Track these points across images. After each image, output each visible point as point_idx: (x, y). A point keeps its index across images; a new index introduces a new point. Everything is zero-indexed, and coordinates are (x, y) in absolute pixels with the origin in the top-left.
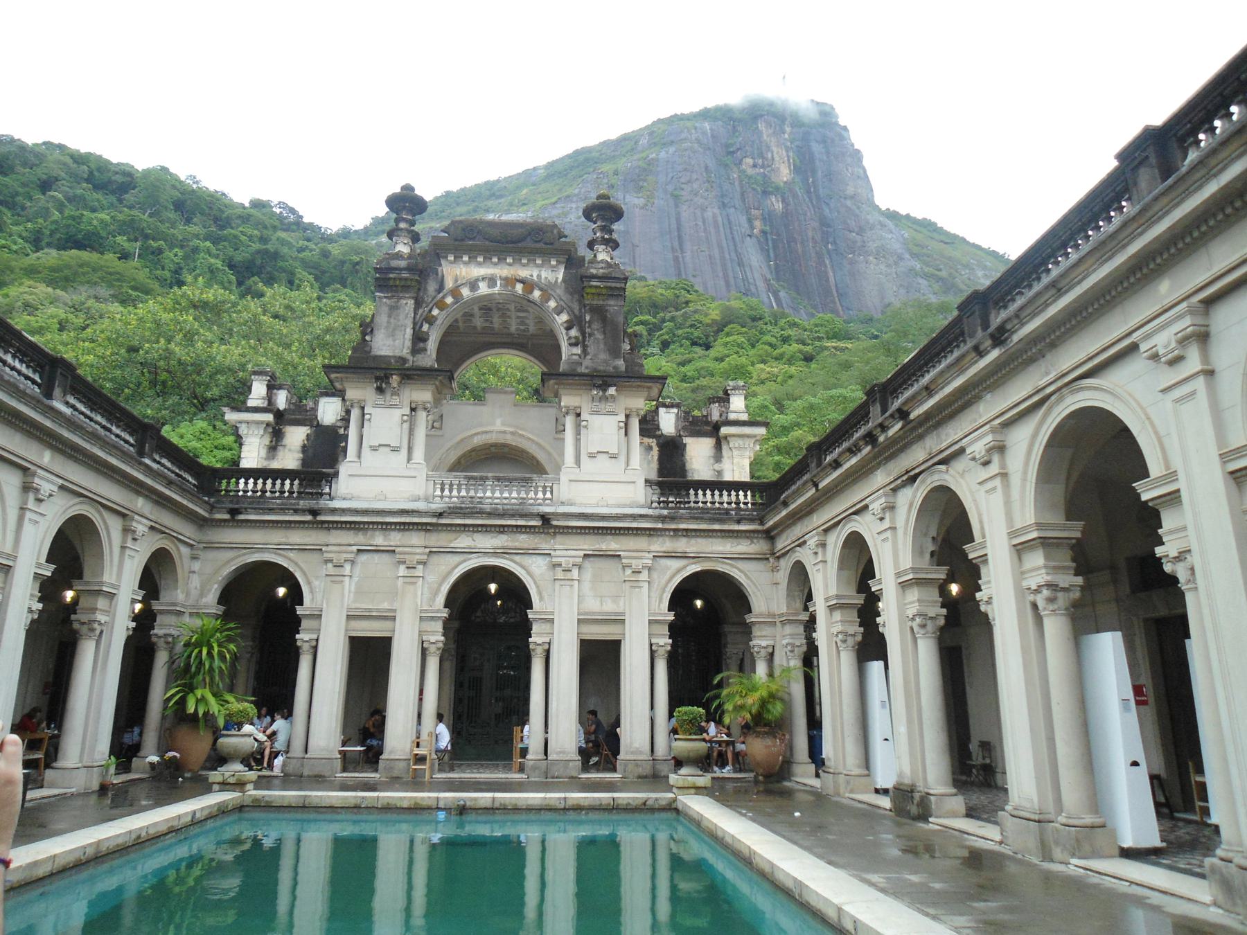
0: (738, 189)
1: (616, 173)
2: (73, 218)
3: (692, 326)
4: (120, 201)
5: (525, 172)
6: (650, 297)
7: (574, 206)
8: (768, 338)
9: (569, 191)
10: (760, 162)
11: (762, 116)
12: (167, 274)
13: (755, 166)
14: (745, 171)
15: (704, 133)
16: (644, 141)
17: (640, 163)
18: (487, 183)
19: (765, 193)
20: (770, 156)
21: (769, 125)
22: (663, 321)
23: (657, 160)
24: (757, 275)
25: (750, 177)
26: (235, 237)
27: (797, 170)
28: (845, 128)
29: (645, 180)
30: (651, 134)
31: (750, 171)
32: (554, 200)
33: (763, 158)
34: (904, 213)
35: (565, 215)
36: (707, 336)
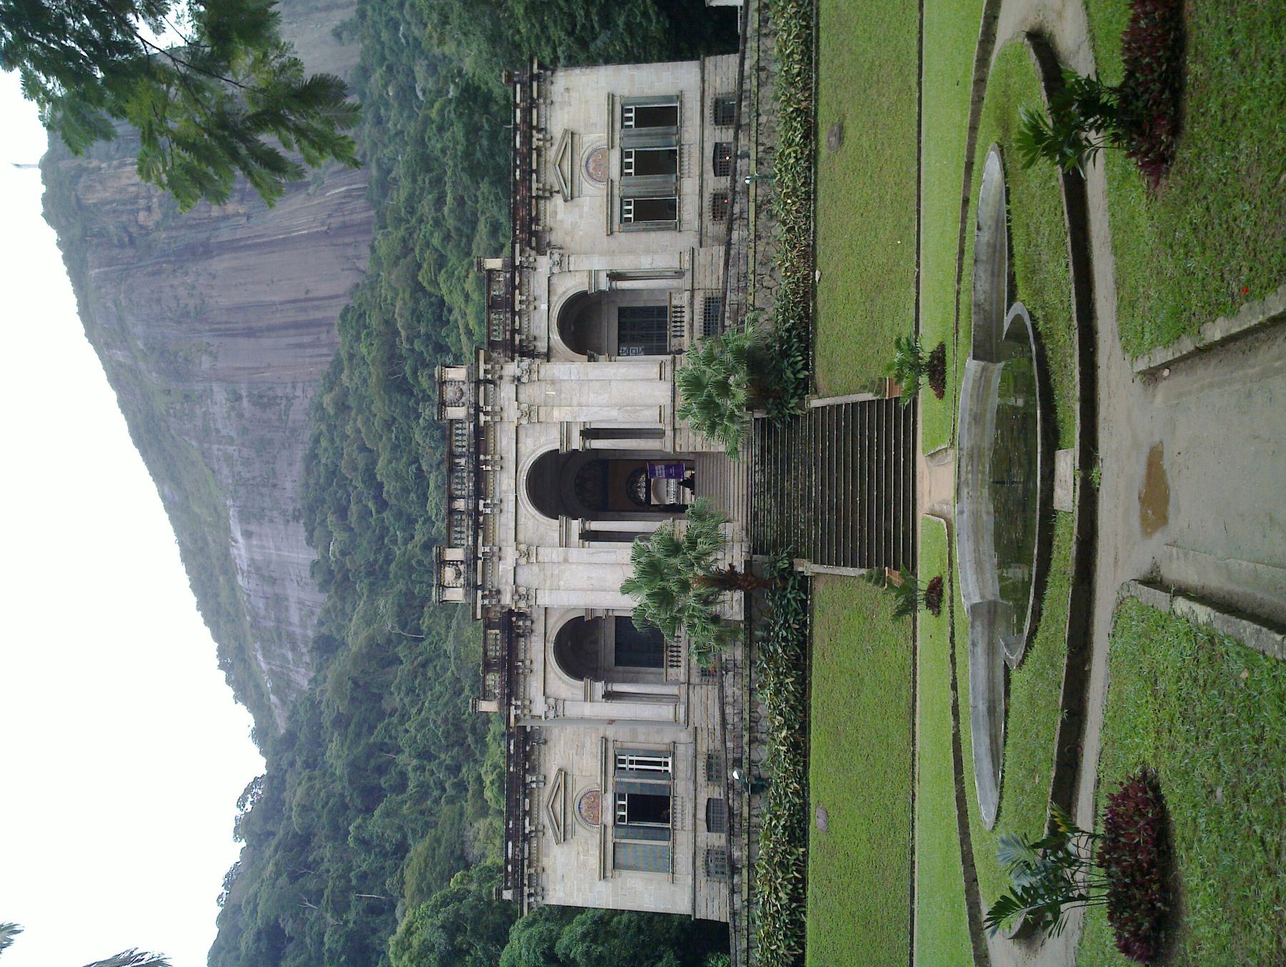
0: (183, 232)
1: (168, 392)
2: (331, 959)
4: (291, 939)
5: (168, 509)
6: (384, 363)
7: (215, 447)
8: (436, 241)
10: (142, 202)
12: (389, 863)
13: (149, 209)
14: (158, 224)
16: (120, 355)
18: (185, 559)
20: (132, 189)
21: (89, 188)
22: (412, 350)
25: (165, 216)
26: (330, 811)
29: (176, 354)
30: (108, 345)
31: (157, 215)
32: (208, 472)
33: (137, 197)
35: (228, 458)
36: (431, 304)
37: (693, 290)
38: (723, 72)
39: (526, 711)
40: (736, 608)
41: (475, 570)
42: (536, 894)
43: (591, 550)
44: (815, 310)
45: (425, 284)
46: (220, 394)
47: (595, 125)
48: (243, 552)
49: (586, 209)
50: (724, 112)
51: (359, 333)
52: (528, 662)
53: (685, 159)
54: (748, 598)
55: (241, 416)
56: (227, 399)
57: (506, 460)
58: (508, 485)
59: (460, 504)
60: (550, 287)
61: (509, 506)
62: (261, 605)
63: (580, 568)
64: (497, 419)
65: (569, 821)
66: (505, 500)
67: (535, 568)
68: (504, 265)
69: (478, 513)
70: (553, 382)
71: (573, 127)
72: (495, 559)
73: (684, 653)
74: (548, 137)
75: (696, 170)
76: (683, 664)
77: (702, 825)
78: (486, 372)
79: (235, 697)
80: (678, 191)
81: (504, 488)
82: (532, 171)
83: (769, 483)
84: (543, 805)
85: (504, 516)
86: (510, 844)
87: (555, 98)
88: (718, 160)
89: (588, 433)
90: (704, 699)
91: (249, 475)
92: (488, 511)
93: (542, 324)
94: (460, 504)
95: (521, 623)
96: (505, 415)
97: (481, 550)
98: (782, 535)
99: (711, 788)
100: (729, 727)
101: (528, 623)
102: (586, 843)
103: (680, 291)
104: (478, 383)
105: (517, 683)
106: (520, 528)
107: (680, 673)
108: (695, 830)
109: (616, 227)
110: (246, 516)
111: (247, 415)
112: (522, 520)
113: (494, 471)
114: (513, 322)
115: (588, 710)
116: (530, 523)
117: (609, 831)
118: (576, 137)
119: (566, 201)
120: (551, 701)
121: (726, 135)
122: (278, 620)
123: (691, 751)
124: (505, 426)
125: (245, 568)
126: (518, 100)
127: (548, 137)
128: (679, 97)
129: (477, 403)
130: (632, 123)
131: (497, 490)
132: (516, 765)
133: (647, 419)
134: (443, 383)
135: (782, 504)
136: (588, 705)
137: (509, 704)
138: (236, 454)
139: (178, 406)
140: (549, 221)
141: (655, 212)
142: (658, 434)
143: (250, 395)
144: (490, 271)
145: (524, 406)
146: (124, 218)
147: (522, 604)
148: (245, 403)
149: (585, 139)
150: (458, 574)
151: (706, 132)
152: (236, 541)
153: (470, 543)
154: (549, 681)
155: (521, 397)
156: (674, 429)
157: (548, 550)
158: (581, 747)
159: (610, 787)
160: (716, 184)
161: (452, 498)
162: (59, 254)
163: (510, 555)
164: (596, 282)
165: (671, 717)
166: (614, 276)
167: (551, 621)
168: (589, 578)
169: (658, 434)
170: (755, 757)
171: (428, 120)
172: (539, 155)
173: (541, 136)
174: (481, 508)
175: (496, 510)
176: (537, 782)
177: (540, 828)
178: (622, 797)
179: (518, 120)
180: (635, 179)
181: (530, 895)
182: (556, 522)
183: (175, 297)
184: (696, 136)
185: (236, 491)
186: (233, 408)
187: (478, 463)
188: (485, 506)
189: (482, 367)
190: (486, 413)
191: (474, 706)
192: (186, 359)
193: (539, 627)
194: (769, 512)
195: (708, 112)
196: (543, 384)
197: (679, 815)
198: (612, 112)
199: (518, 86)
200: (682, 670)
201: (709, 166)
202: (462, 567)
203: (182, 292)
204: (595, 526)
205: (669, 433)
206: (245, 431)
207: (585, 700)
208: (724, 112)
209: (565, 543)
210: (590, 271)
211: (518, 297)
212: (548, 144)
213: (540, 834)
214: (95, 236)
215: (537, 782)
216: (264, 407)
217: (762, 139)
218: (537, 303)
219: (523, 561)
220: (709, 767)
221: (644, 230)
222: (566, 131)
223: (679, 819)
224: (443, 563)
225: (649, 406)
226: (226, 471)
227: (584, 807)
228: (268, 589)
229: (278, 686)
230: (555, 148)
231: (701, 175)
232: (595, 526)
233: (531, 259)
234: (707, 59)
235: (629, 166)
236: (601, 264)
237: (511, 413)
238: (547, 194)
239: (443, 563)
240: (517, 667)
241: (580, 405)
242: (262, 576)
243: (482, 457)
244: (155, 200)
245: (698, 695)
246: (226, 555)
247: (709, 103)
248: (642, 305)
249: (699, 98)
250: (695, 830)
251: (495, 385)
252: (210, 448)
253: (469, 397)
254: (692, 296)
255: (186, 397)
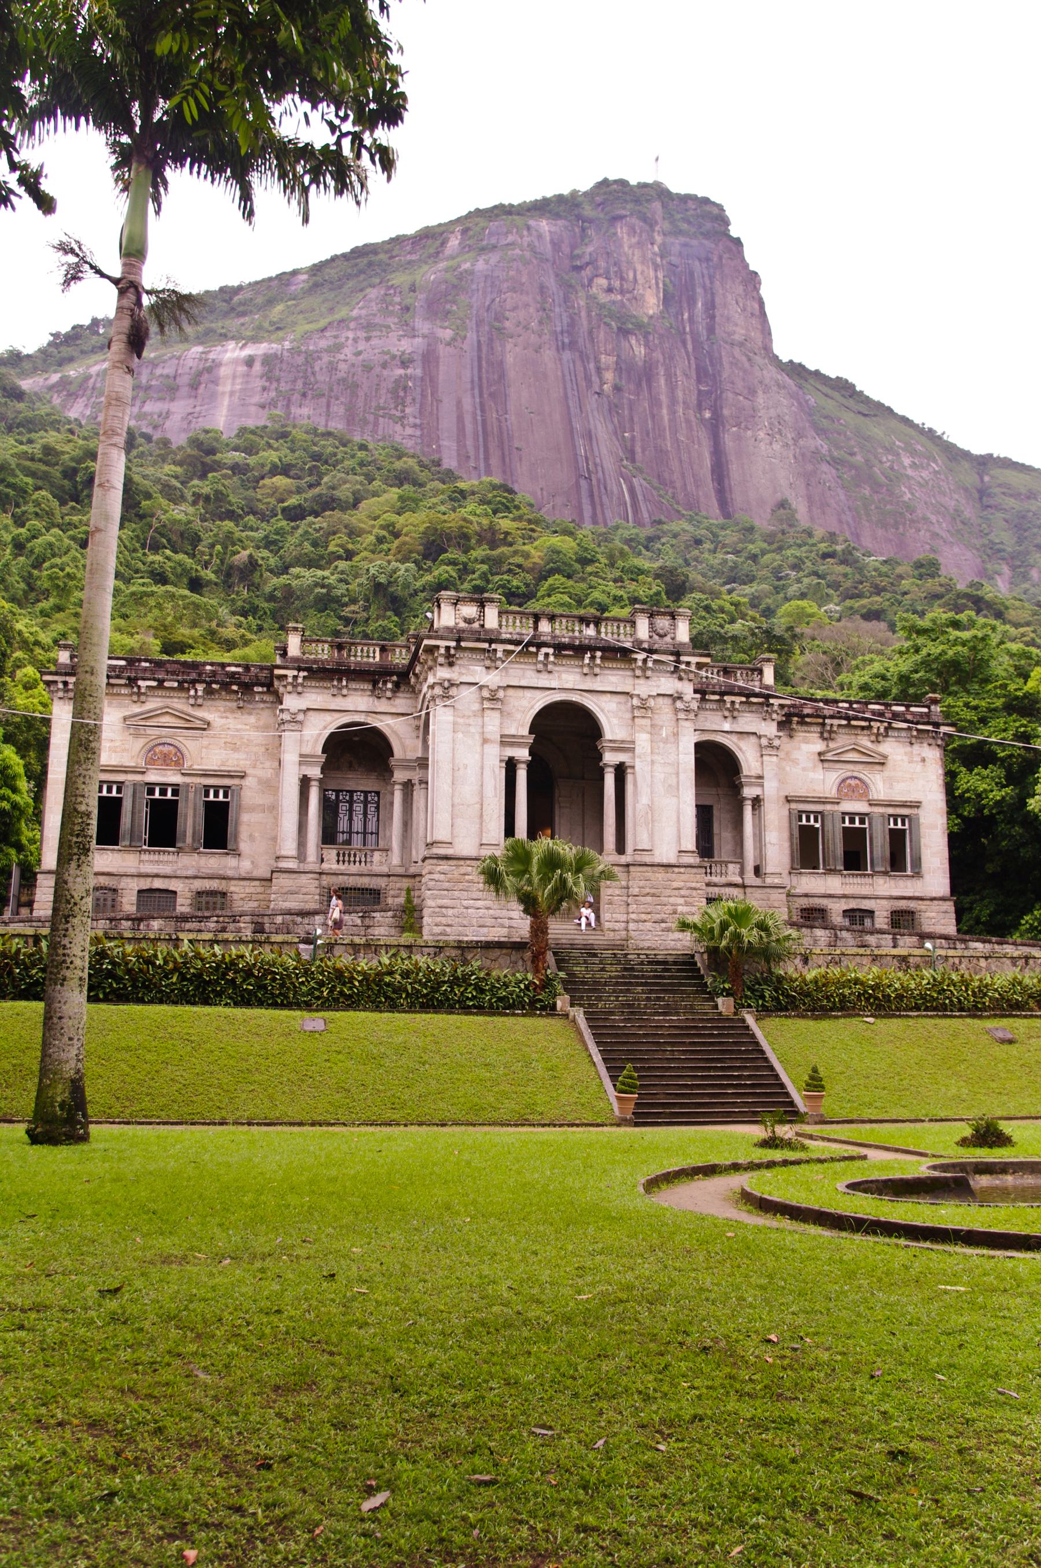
1: (413, 289)
3: (510, 571)
7: (351, 335)
9: (342, 313)
11: (621, 218)
13: (610, 290)
15: (540, 237)
17: (448, 276)
19: (623, 332)
21: (632, 231)
23: (470, 272)
24: (604, 451)
25: (602, 306)
27: (667, 300)
28: (738, 242)
29: (454, 302)
31: (604, 298)
32: (323, 323)
33: (622, 279)
34: (812, 368)
35: (338, 348)
37: (744, 886)
38: (941, 919)
39: (290, 688)
40: (437, 930)
41: (478, 640)
42: (66, 690)
43: (497, 770)
44: (836, 1017)
45: (550, 581)
46: (406, 346)
47: (891, 787)
48: (228, 356)
49: (811, 775)
50: (903, 920)
51: (489, 503)
52: (345, 691)
53: (859, 880)
54: (518, 947)
55: (384, 365)
56: (403, 353)
57: (594, 679)
58: (566, 682)
59: (544, 626)
60: (748, 735)
61: (544, 681)
62: (166, 371)
63: (477, 757)
64: (638, 672)
65: (149, 731)
66: (551, 676)
67: (476, 707)
68: (767, 687)
69: (539, 646)
70: (676, 735)
71: (890, 763)
72: (488, 663)
73: (354, 868)
74: (881, 738)
75: (849, 890)
76: (342, 867)
77: (145, 884)
78: (688, 664)
79: (56, 335)
80: (830, 871)
81: (564, 676)
82: (848, 718)
83: (632, 969)
84: (168, 702)
85: (534, 674)
86: (123, 663)
87: (916, 747)
88: (858, 914)
89: (621, 771)
90: (304, 890)
91: (317, 369)
92: (541, 658)
93: (719, 726)
94: (544, 626)
95: (389, 685)
96: (642, 681)
97: (500, 648)
98: (583, 983)
99: (189, 895)
100: (299, 919)
101: (389, 694)
102: (124, 750)
103: (742, 873)
104: (677, 654)
105: (322, 679)
106: (520, 693)
107: (331, 864)
108: (140, 876)
109: (794, 806)
110: (269, 360)
111: (385, 373)
112: (528, 694)
113: (582, 667)
114: (714, 693)
115: (290, 758)
116: (525, 703)
117: (138, 778)
118: (878, 767)
119: (820, 754)
120: (300, 717)
121: (881, 921)
122: (149, 388)
123: (230, 873)
124: (630, 681)
125: (211, 356)
126: (912, 709)
127: (881, 738)
128: (917, 874)
129: (655, 652)
130: (804, 822)
131: (561, 669)
132: (214, 673)
133: (637, 836)
134: (673, 616)
135: (617, 984)
136: (296, 759)
137: (299, 669)
138: (342, 357)
139: (397, 299)
140: (800, 735)
141: (807, 849)
142: (621, 849)
143: (408, 377)
144: (761, 672)
145: (651, 703)
146: (602, 264)
147: (438, 691)
148: (401, 372)
149: (878, 776)
150: (469, 621)
151: (884, 902)
152: (241, 348)
153: (504, 636)
154: (322, 714)
155: (660, 700)
156: (628, 865)
157: (497, 722)
158: (235, 749)
159: (188, 780)
160: (836, 909)
161: (552, 618)
162: (566, 191)
163: (492, 679)
164: (751, 784)
165: (284, 853)
166: (757, 801)
167: (390, 721)
168: (466, 767)
169: (621, 849)
170: (338, 951)
171: (715, 595)
172: (863, 728)
173: (882, 730)
174: (544, 650)
175: (540, 666)
176: (196, 697)
177: (143, 698)
178: (175, 793)
179: (894, 708)
180: (839, 827)
181: (65, 683)
182: (525, 731)
183: (515, 309)
184: (880, 891)
185: (299, 353)
186: (394, 357)
187: (593, 649)
188: (547, 655)
189: (694, 660)
190: (645, 661)
191: (296, 629)
192: (449, 312)
193: (382, 706)
194: (603, 970)
195: (903, 904)
196: (673, 723)
197: (156, 857)
198: (904, 805)
199: (925, 710)
200: (335, 866)
201: (853, 904)
202: (476, 625)
203: (522, 314)
204: (522, 775)
205: (623, 859)
206: (368, 368)
207: (301, 756)
208: (903, 920)
209: (506, 741)
210: (761, 777)
211: (738, 699)
212: (873, 738)
213: (135, 698)
214: (583, 230)
215: (196, 697)
216: (394, 392)
217: (965, 961)
218: (729, 719)
219: (486, 693)
220: (212, 893)
221: (791, 835)
222: (885, 757)
223: (152, 857)
224: (482, 604)
225: (651, 836)
226: (323, 344)
227: (166, 749)
228: (184, 380)
229: (71, 383)
230: (869, 745)
231: (845, 896)
232: (522, 775)
233: (774, 716)
234: (952, 903)
235: (852, 821)
236: (771, 790)
237: (643, 688)
238: (826, 735)
239: (482, 604)
240: (340, 680)
241: (653, 762)
242: (200, 374)
243: (599, 654)
244: (619, 297)
245: (308, 883)
246: (225, 337)
247: (912, 905)
248: (716, 830)
249: (917, 894)
250: (140, 876)
251: (672, 673)
252: (348, 329)
253: (659, 644)
254: (736, 885)
255: (407, 309)
